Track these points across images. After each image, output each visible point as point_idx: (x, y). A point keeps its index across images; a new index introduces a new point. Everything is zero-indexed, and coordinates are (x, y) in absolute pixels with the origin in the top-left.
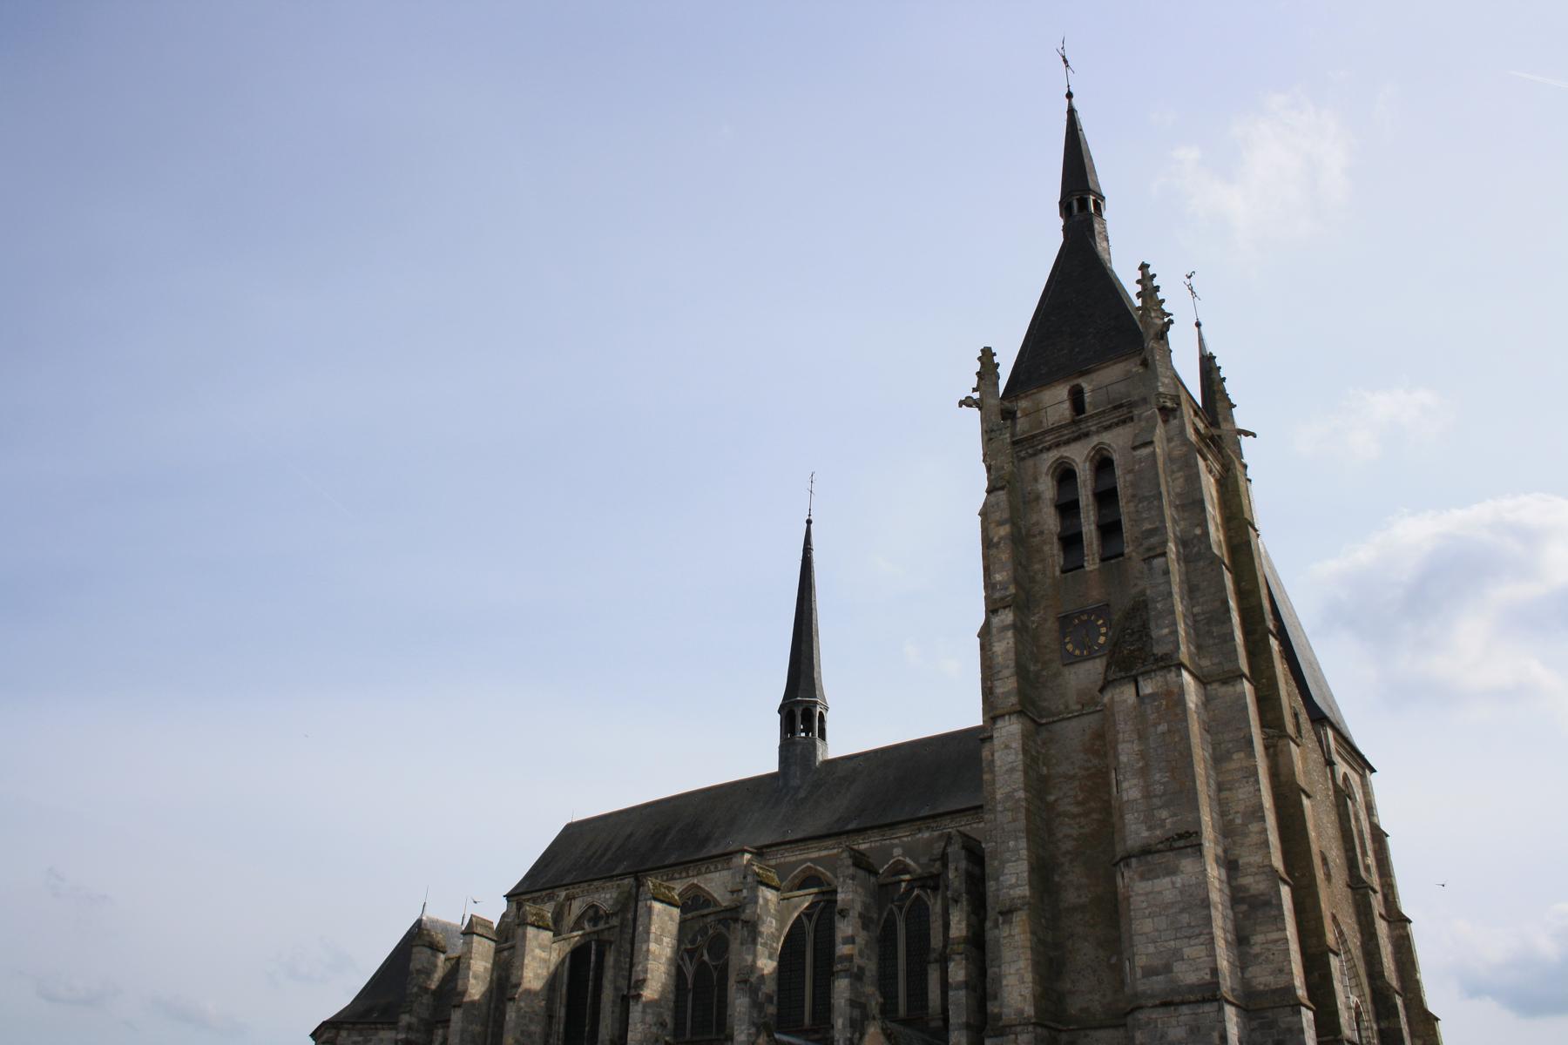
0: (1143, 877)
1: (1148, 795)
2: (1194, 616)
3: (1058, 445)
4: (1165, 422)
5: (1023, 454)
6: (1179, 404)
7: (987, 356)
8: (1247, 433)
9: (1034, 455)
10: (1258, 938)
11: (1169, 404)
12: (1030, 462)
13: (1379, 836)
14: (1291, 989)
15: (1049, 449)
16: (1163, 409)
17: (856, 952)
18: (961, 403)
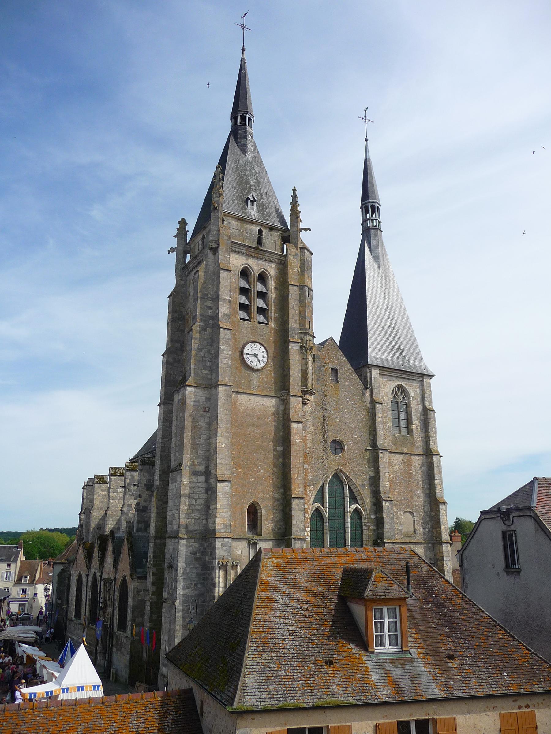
0: (172, 483)
1: (176, 446)
2: (212, 354)
3: (194, 268)
4: (214, 254)
5: (186, 274)
6: (219, 245)
7: (183, 223)
8: (306, 230)
9: (189, 273)
10: (211, 507)
11: (214, 245)
12: (189, 277)
13: (427, 414)
14: (214, 531)
15: (192, 270)
16: (211, 249)
17: (142, 500)
18: (169, 252)
